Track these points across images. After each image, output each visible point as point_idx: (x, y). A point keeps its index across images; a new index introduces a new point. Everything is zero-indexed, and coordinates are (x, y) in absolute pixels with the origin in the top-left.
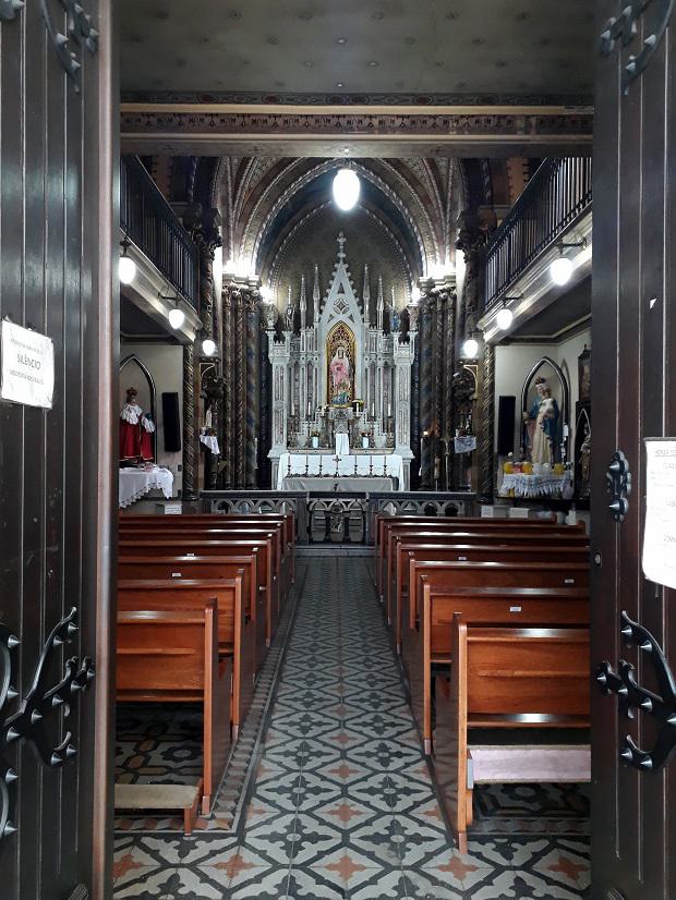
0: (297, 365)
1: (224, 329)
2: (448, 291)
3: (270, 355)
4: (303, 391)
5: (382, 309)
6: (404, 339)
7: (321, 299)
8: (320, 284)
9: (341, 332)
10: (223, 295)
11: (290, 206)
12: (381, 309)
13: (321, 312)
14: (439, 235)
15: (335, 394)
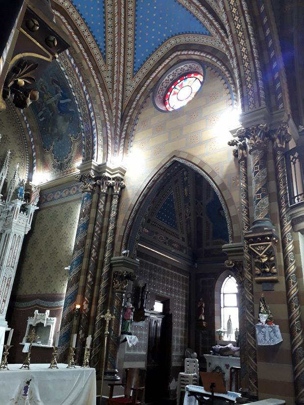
2: (118, 179)
6: (24, 209)
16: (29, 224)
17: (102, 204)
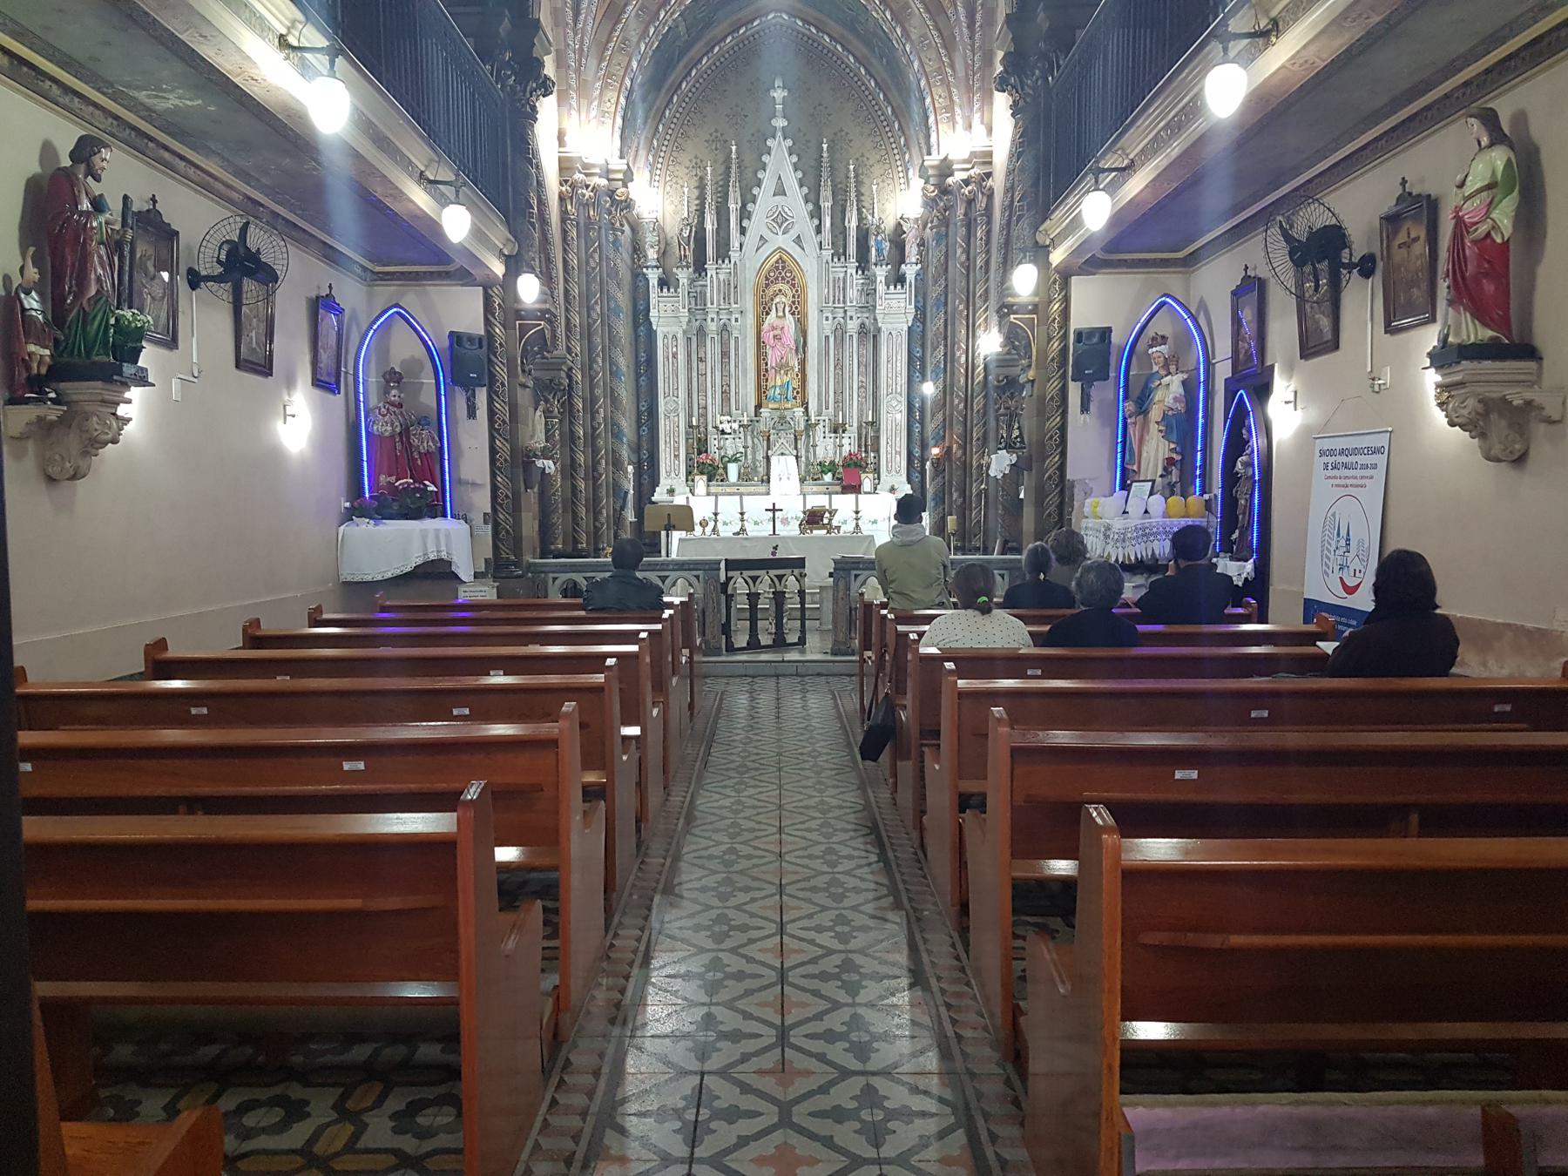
0: (701, 333)
1: (565, 262)
3: (653, 313)
4: (713, 380)
5: (854, 224)
7: (744, 206)
9: (781, 271)
10: (562, 198)
11: (682, 29)
12: (852, 223)
13: (743, 231)
14: (961, 73)
15: (770, 384)
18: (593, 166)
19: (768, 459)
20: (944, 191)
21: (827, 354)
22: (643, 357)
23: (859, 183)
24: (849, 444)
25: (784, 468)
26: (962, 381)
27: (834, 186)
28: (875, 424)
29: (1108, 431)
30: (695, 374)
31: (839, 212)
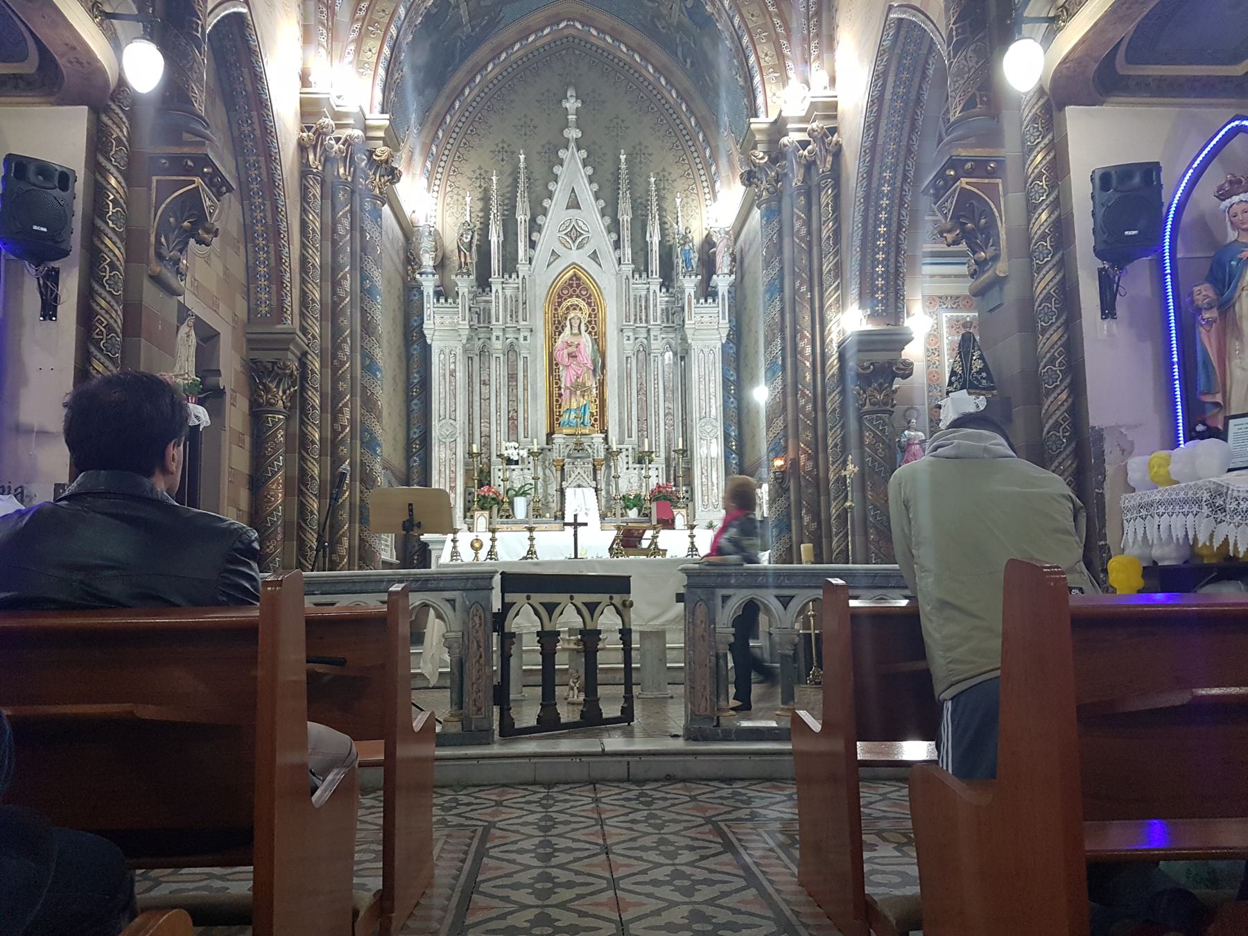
0: (484, 353)
1: (304, 225)
3: (428, 325)
4: (499, 404)
5: (656, 239)
6: (707, 292)
7: (533, 220)
8: (529, 189)
10: (302, 147)
12: (655, 239)
13: (533, 245)
15: (565, 407)
16: (724, 318)
17: (799, 218)
18: (346, 115)
19: (562, 492)
20: (777, 155)
21: (629, 376)
22: (416, 378)
23: (661, 199)
24: (656, 476)
25: (582, 501)
26: (808, 377)
27: (633, 200)
28: (687, 452)
29: (1148, 350)
30: (476, 398)
31: (640, 226)
